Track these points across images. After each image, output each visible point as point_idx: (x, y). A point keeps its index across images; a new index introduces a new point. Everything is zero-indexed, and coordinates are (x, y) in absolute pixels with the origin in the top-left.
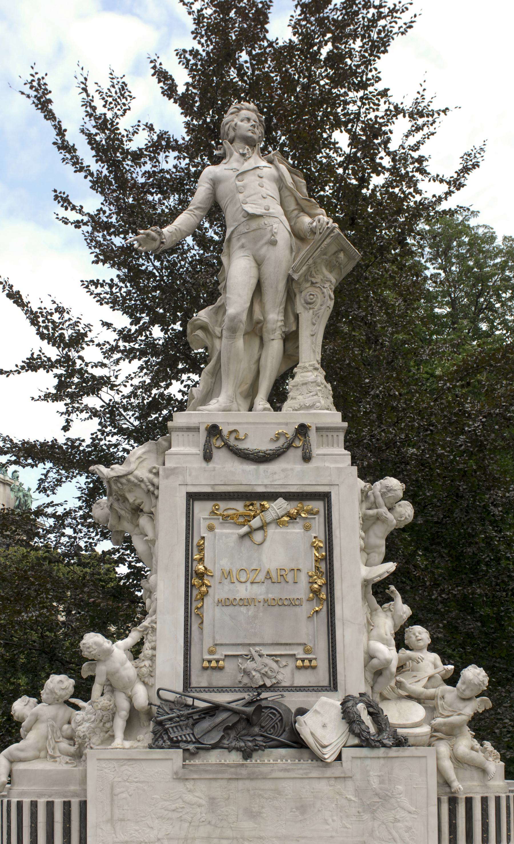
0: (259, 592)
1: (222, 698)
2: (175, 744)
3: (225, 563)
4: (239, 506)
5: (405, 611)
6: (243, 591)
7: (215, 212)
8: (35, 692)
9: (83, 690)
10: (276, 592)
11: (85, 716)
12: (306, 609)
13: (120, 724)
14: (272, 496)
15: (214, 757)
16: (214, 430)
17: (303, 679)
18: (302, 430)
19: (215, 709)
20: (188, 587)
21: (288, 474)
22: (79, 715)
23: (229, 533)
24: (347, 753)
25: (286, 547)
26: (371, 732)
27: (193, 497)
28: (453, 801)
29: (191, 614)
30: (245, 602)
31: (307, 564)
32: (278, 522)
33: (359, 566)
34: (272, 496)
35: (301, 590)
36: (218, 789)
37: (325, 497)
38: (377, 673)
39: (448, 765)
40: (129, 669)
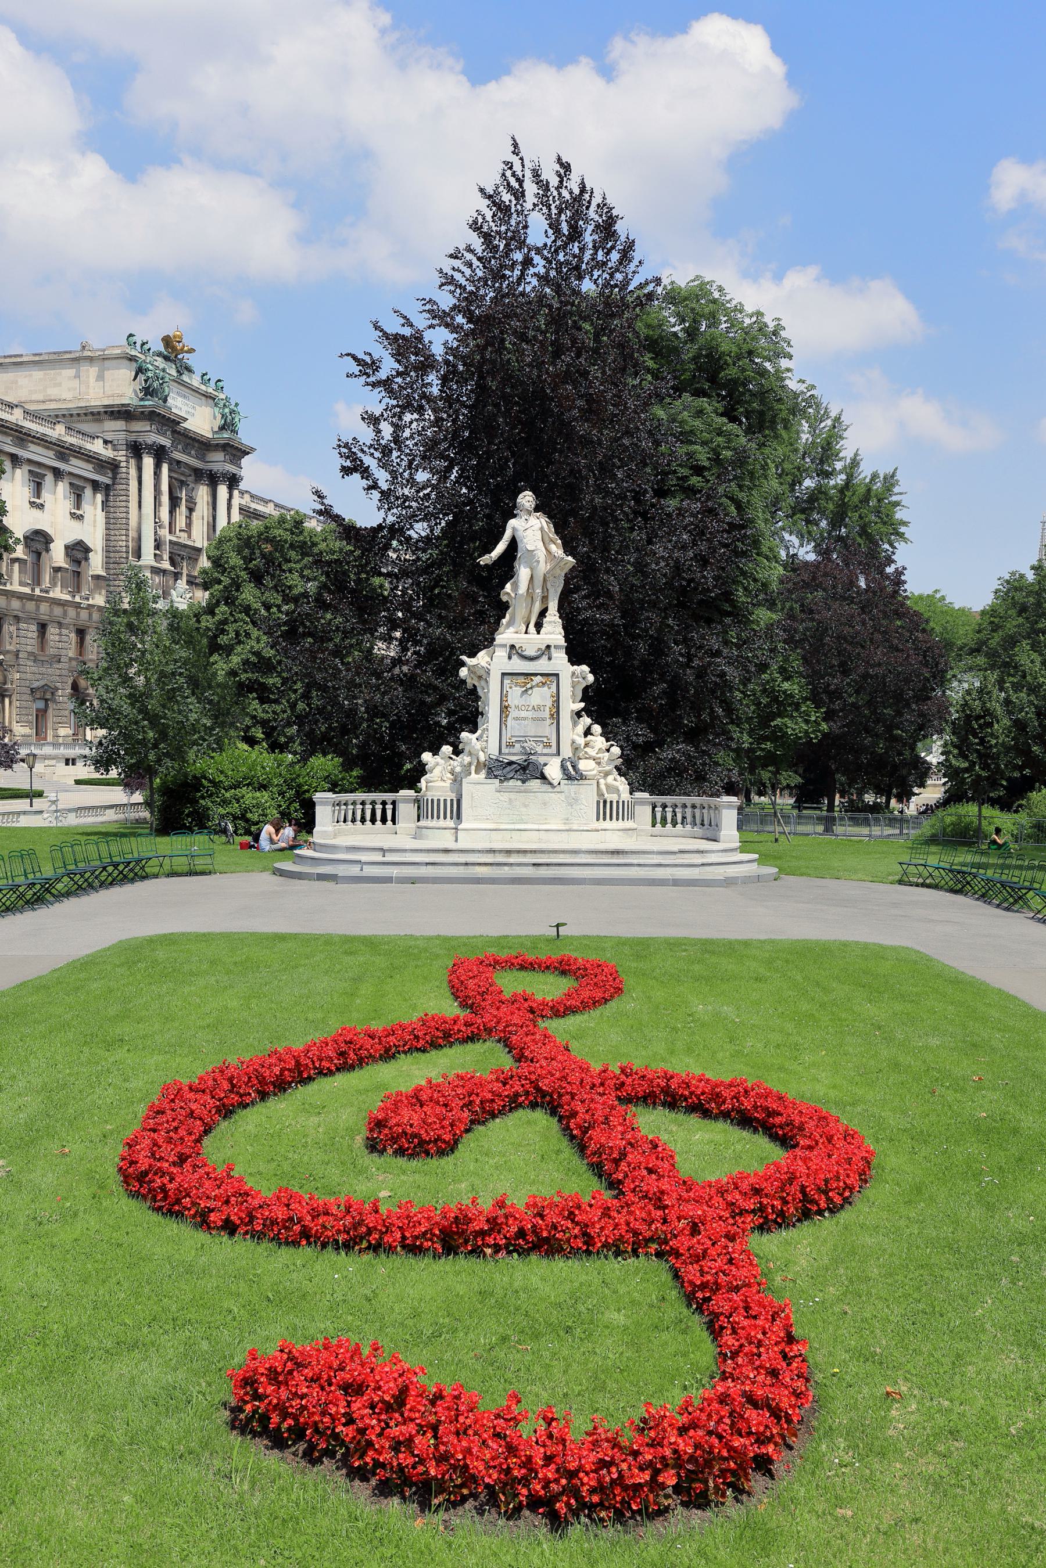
0: (529, 714)
1: (514, 758)
2: (496, 777)
3: (516, 703)
4: (521, 680)
5: (589, 721)
6: (523, 714)
7: (513, 544)
8: (435, 751)
9: (457, 752)
10: (536, 715)
11: (457, 763)
12: (549, 722)
13: (473, 768)
14: (536, 675)
15: (512, 783)
16: (513, 647)
17: (546, 751)
18: (548, 647)
19: (511, 763)
20: (501, 712)
21: (542, 665)
22: (456, 763)
23: (519, 690)
24: (563, 782)
25: (541, 696)
26: (572, 774)
27: (503, 674)
28: (605, 802)
29: (503, 722)
30: (525, 719)
31: (549, 703)
32: (537, 685)
33: (571, 704)
34: (536, 675)
35: (547, 714)
36: (513, 796)
37: (557, 675)
38: (576, 749)
39: (603, 787)
40: (478, 745)
